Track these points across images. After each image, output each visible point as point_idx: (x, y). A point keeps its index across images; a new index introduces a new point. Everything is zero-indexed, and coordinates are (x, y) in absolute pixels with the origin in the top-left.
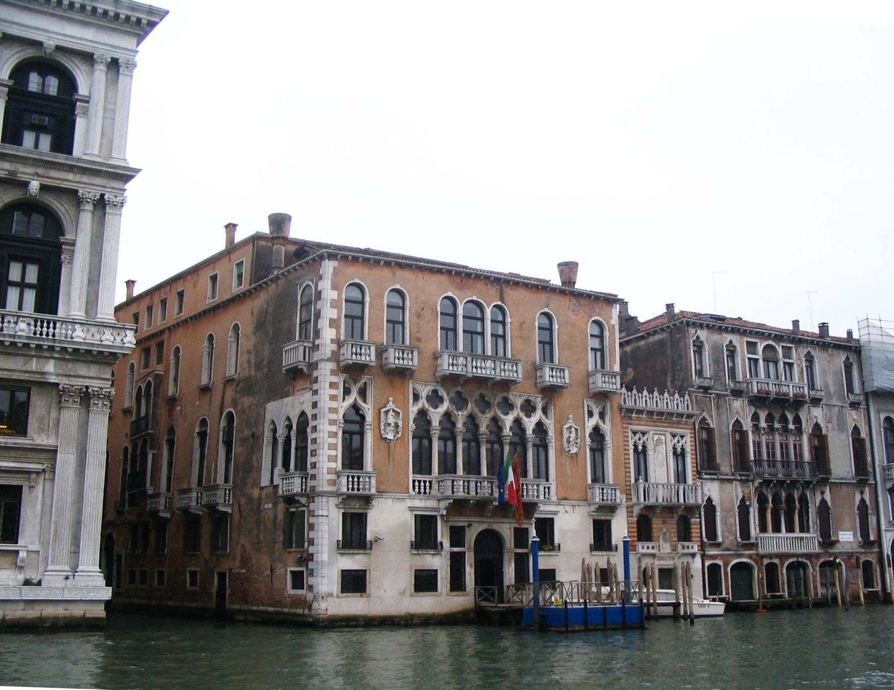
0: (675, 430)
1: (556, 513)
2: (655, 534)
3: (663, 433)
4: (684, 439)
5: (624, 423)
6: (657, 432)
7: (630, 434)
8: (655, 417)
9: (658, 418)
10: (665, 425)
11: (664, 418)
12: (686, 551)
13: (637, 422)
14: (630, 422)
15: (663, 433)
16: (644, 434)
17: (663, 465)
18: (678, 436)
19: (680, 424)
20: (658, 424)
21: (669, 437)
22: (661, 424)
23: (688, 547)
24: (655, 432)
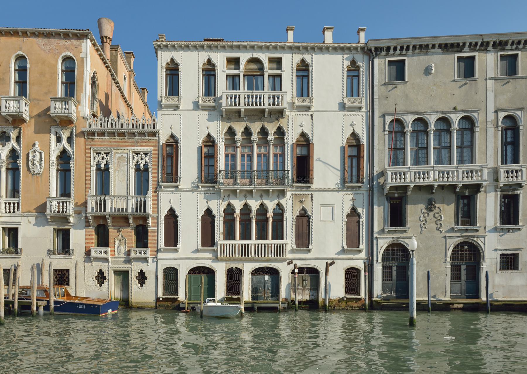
0: (137, 149)
1: (19, 223)
2: (111, 241)
3: (126, 151)
4: (148, 156)
5: (88, 145)
6: (119, 151)
7: (93, 154)
8: (117, 137)
9: (121, 138)
10: (127, 144)
11: (126, 138)
12: (138, 255)
13: (100, 143)
14: (93, 143)
15: (126, 151)
16: (107, 154)
17: (124, 180)
18: (142, 153)
19: (142, 142)
20: (120, 144)
21: (132, 155)
22: (124, 144)
23: (140, 253)
24: (117, 151)
